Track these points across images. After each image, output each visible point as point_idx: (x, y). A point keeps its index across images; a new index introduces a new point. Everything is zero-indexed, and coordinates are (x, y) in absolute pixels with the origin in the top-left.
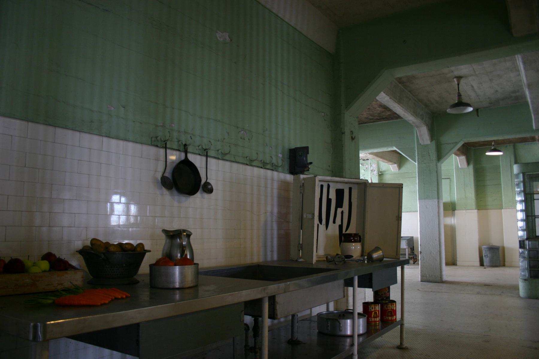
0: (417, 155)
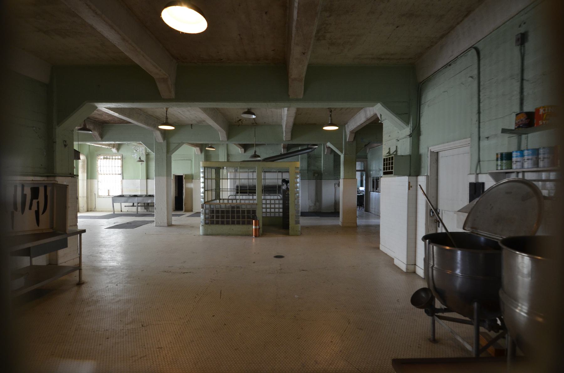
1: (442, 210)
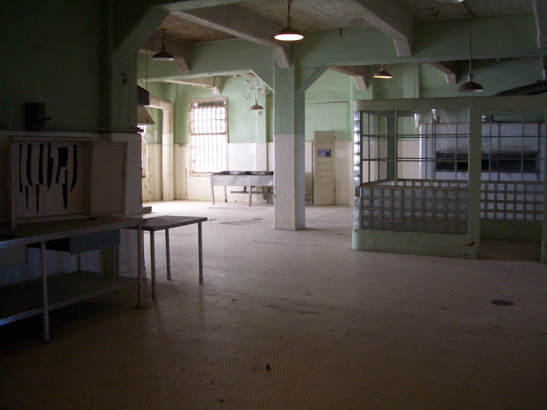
0: (274, 81)
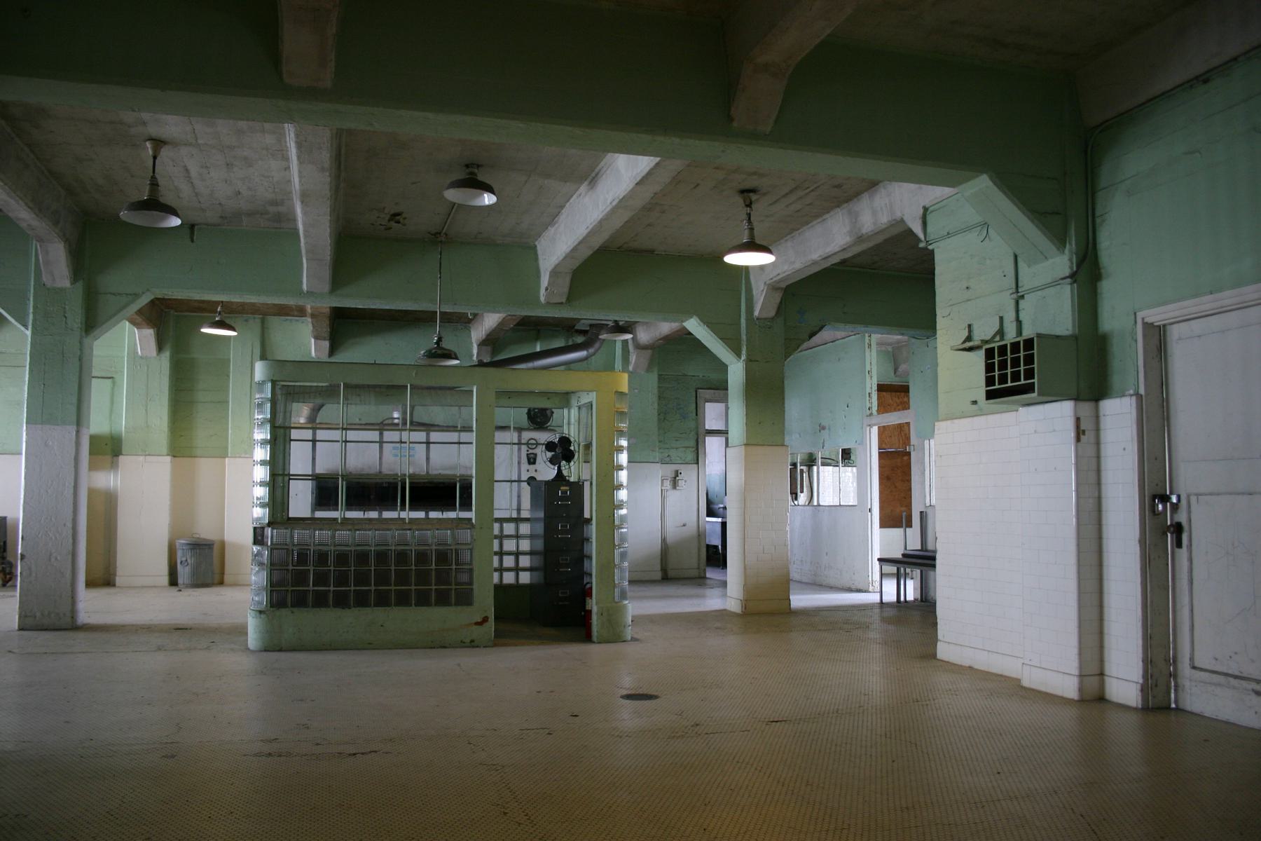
0: (31, 310)
1: (1188, 496)
